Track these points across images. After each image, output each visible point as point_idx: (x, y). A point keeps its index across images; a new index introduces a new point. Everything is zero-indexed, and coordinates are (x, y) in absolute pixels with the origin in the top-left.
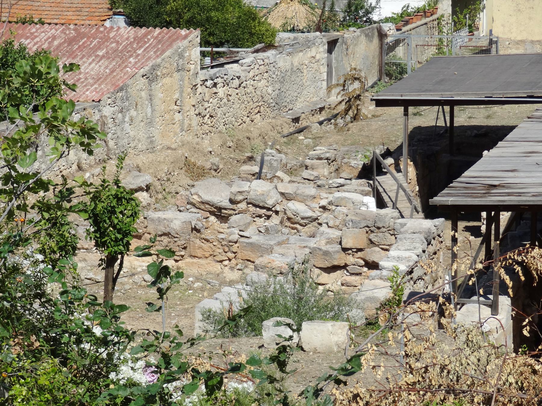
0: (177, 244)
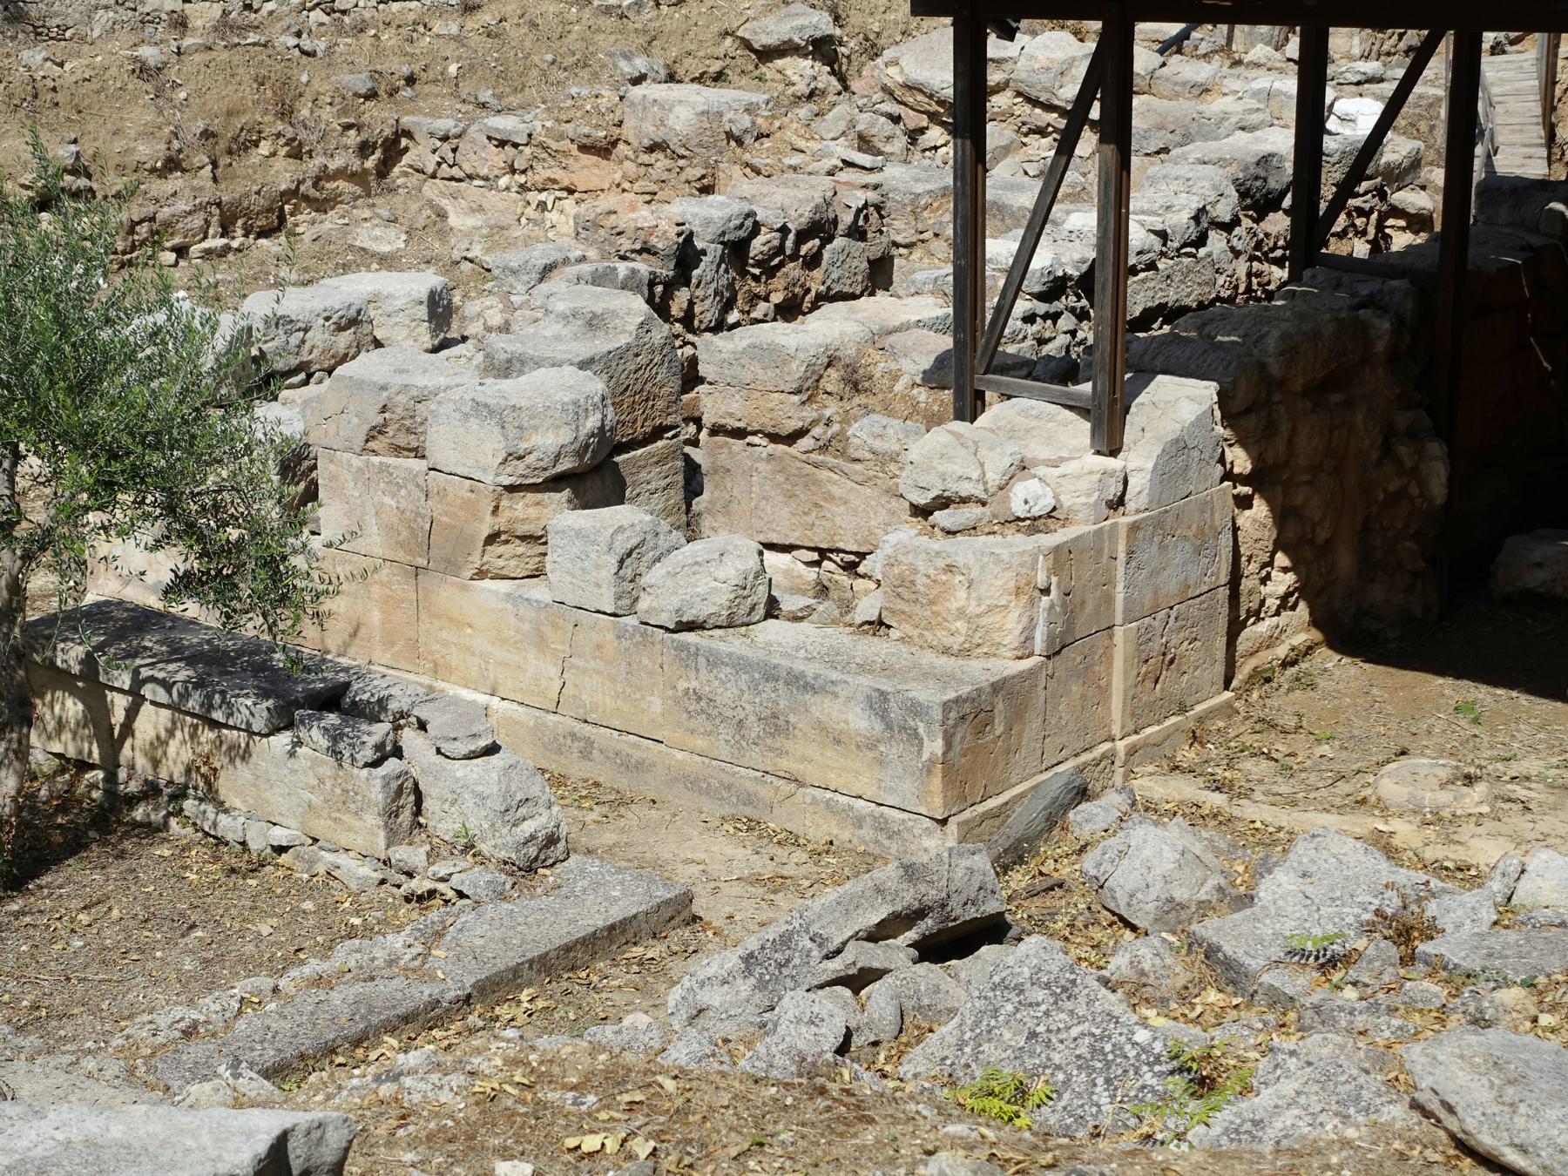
0: (683, 177)
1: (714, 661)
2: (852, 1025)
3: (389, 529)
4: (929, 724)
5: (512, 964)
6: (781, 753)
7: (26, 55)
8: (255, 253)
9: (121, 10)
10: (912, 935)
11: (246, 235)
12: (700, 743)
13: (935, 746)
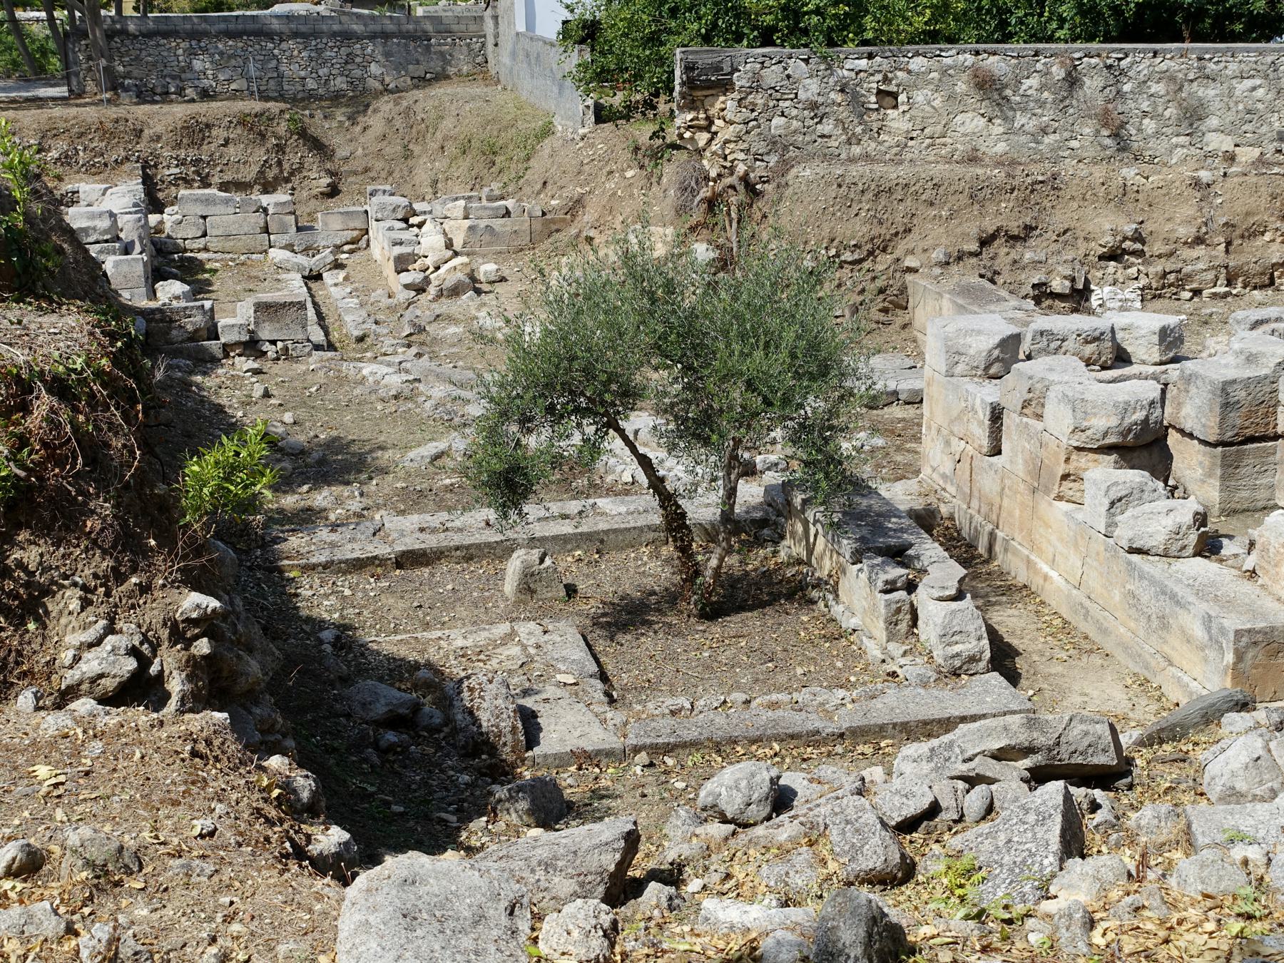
1: (1142, 577)
2: (943, 804)
3: (1026, 461)
4: (1228, 642)
5: (880, 722)
6: (1165, 642)
7: (1125, 171)
8: (1246, 298)
9: (1192, 148)
10: (1027, 762)
11: (1245, 287)
12: (1132, 625)
13: (1230, 658)
